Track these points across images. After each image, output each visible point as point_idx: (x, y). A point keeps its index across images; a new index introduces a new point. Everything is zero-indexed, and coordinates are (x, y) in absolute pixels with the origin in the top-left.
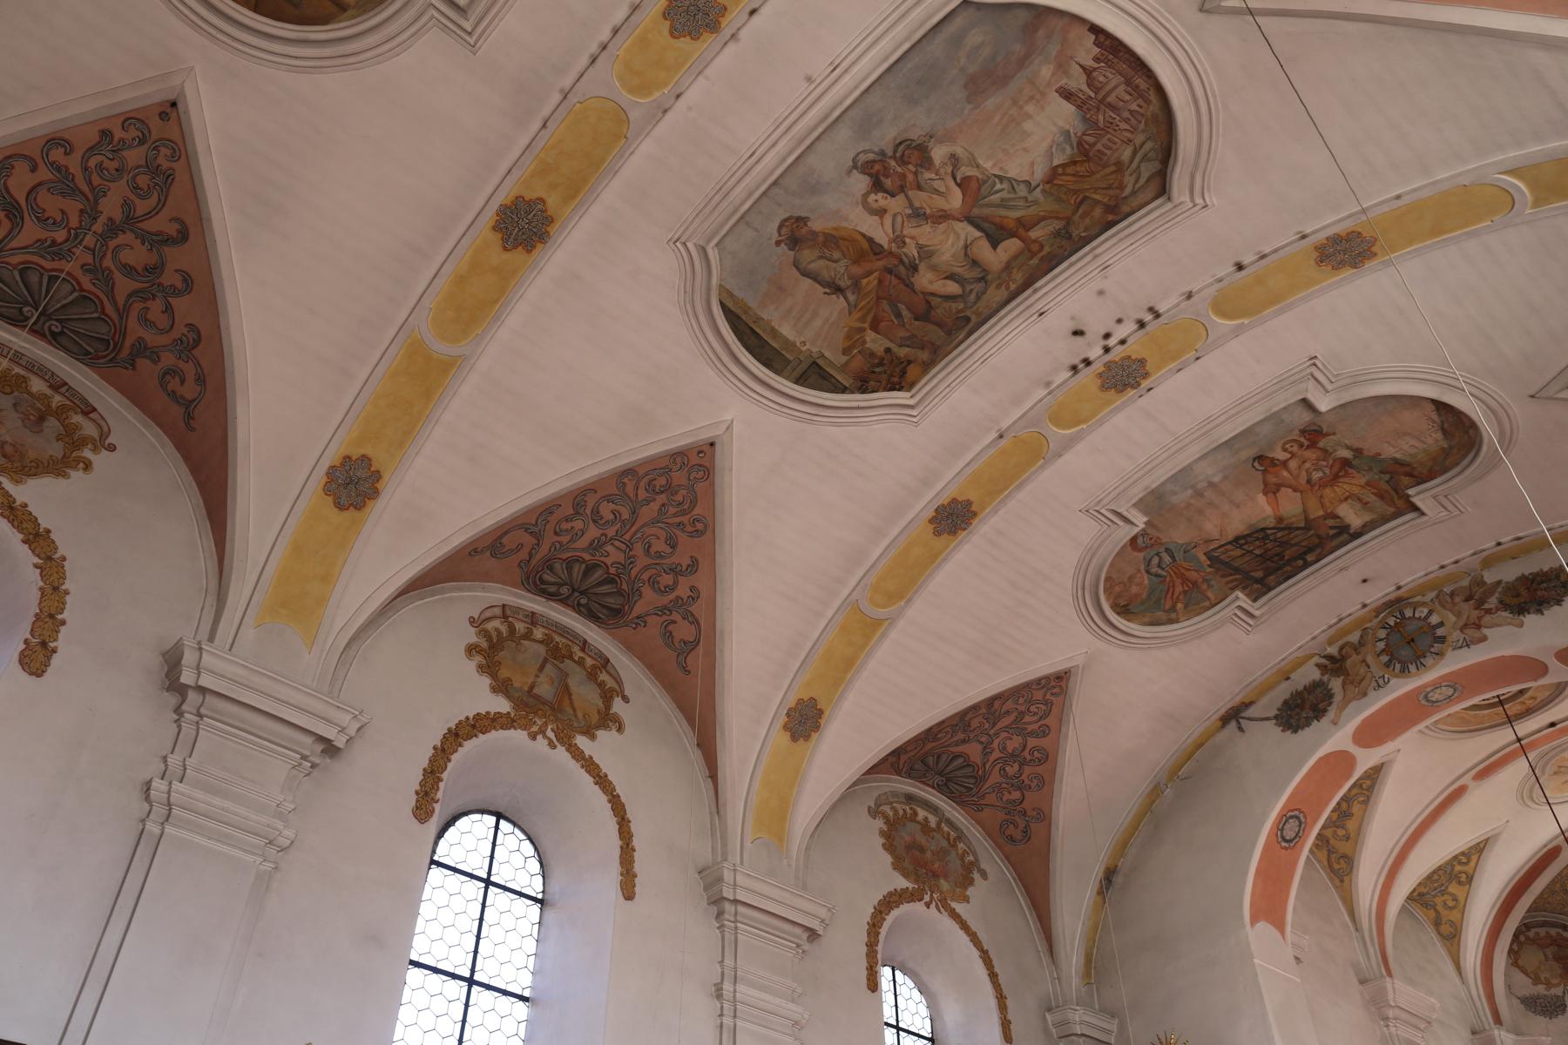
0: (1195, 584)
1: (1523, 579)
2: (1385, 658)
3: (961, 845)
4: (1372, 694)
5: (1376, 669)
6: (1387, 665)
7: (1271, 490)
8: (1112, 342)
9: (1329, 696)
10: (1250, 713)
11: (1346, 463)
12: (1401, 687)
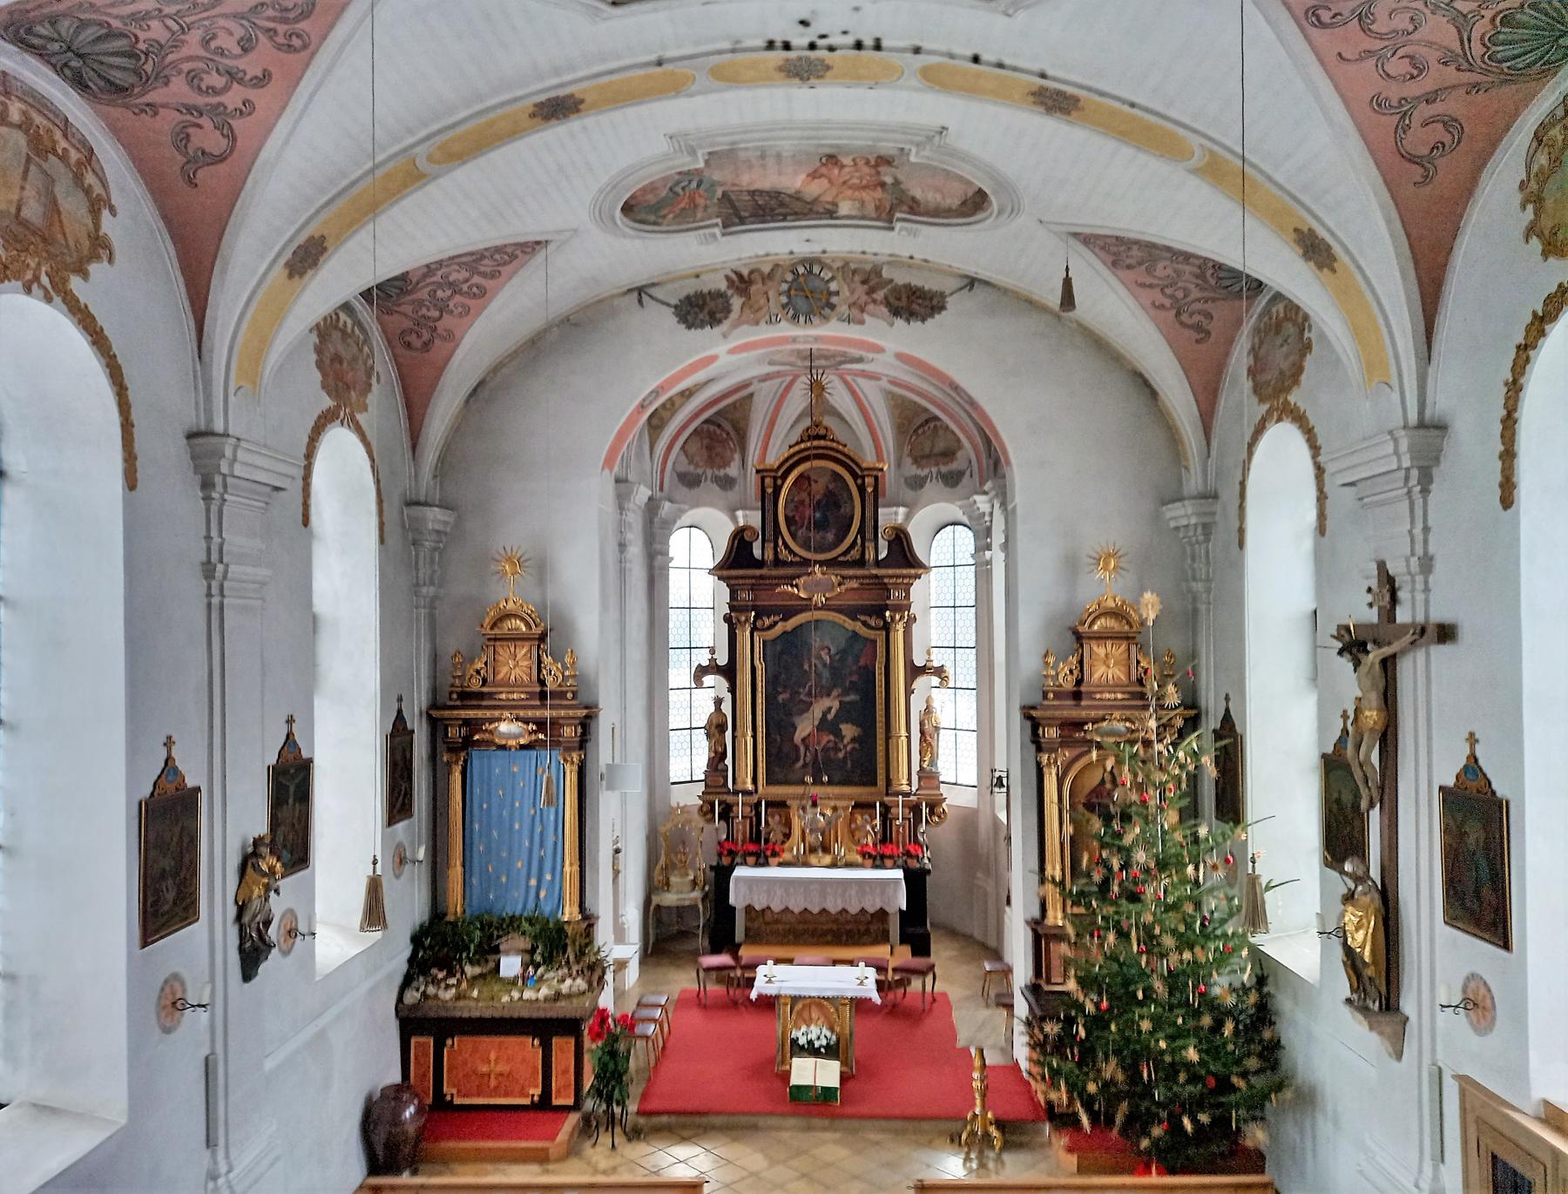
0: (696, 206)
1: (908, 287)
2: (784, 299)
3: (366, 349)
4: (763, 325)
5: (774, 307)
6: (784, 306)
7: (814, 175)
8: (821, 42)
9: (727, 310)
10: (652, 291)
11: (883, 185)
12: (785, 329)
